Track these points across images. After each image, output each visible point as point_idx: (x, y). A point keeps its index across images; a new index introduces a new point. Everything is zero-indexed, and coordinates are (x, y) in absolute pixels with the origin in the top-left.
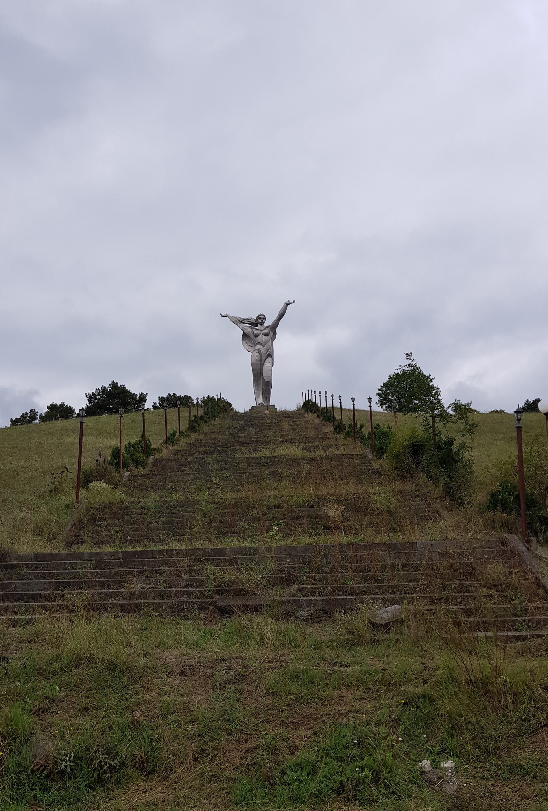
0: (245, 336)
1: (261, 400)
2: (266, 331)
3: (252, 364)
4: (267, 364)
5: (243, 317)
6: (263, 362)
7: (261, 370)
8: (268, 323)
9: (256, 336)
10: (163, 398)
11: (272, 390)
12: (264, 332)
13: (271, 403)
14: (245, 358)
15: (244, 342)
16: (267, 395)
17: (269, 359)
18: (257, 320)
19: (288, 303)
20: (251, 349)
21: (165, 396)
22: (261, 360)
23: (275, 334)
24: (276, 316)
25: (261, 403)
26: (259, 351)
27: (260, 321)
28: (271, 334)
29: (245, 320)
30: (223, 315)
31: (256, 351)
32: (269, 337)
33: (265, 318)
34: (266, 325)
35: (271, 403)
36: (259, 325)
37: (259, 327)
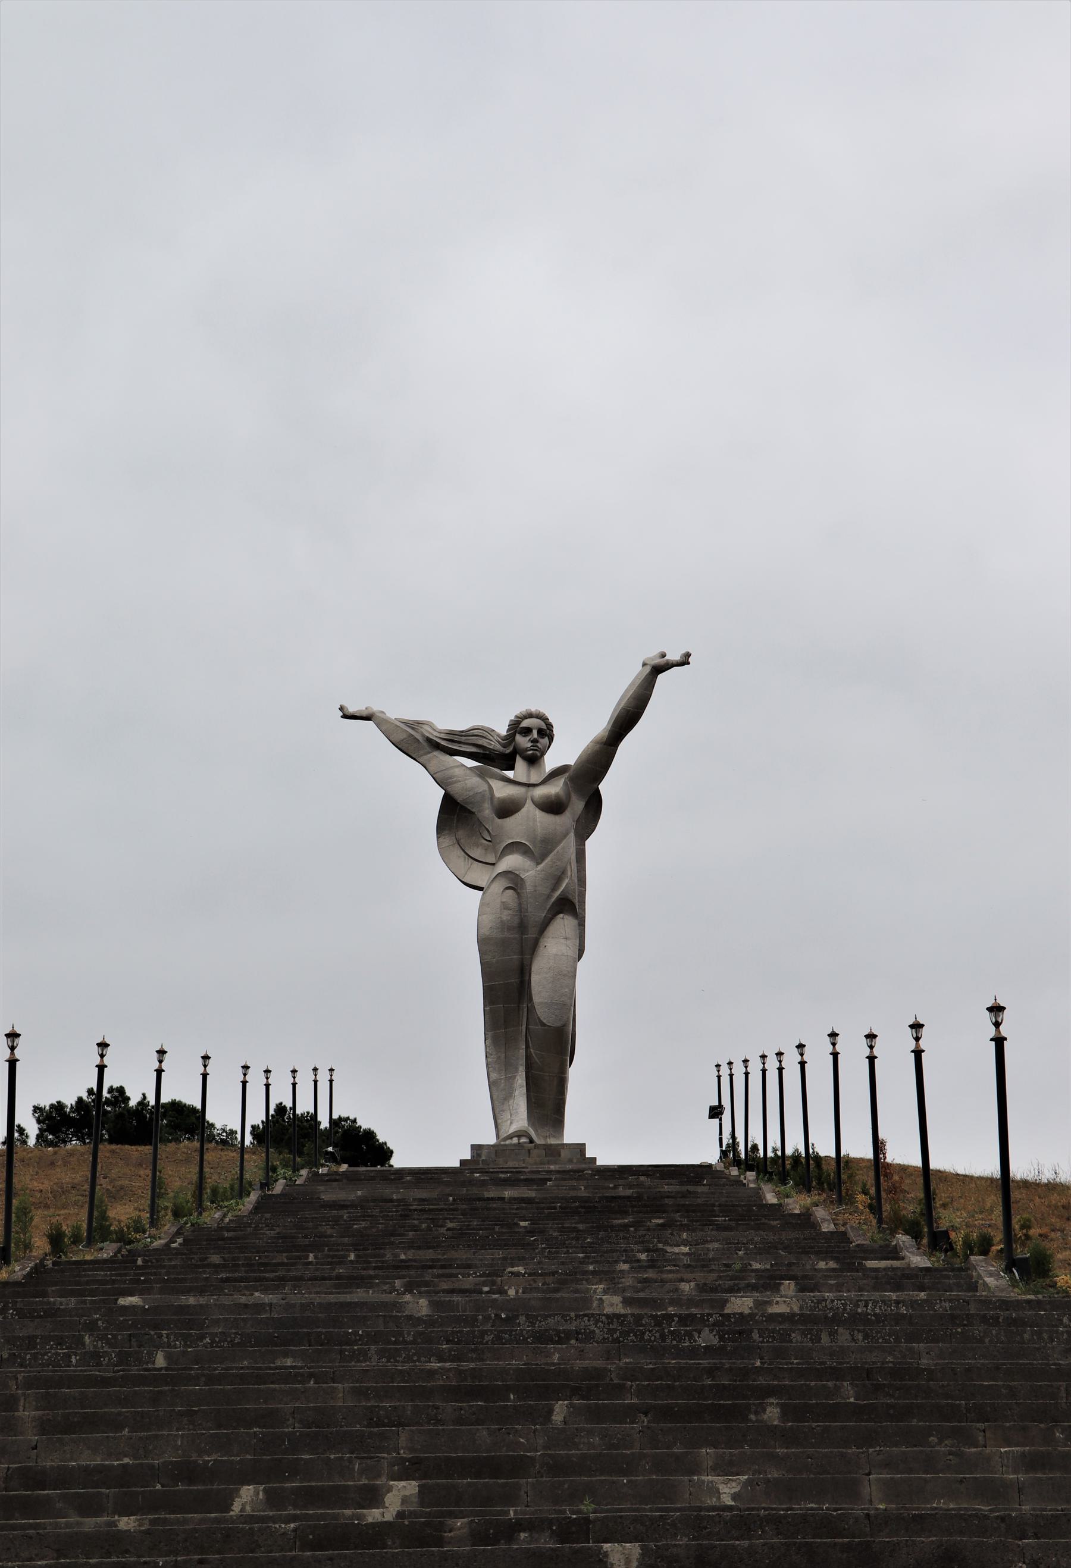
0: (455, 815)
1: (519, 1118)
2: (555, 789)
3: (484, 943)
4: (555, 945)
5: (449, 719)
6: (531, 934)
7: (523, 972)
8: (565, 751)
9: (507, 809)
10: (59, 1107)
11: (574, 1073)
12: (540, 792)
13: (571, 1135)
14: (450, 913)
15: (447, 841)
16: (548, 1101)
17: (564, 924)
18: (510, 738)
19: (659, 661)
20: (481, 875)
21: (70, 1101)
22: (522, 927)
23: (594, 805)
24: (599, 724)
25: (519, 1134)
26: (513, 880)
27: (523, 741)
28: (578, 805)
29: (454, 736)
30: (352, 710)
31: (498, 887)
32: (566, 821)
33: (547, 732)
34: (552, 760)
35: (571, 1135)
36: (520, 763)
37: (520, 771)
